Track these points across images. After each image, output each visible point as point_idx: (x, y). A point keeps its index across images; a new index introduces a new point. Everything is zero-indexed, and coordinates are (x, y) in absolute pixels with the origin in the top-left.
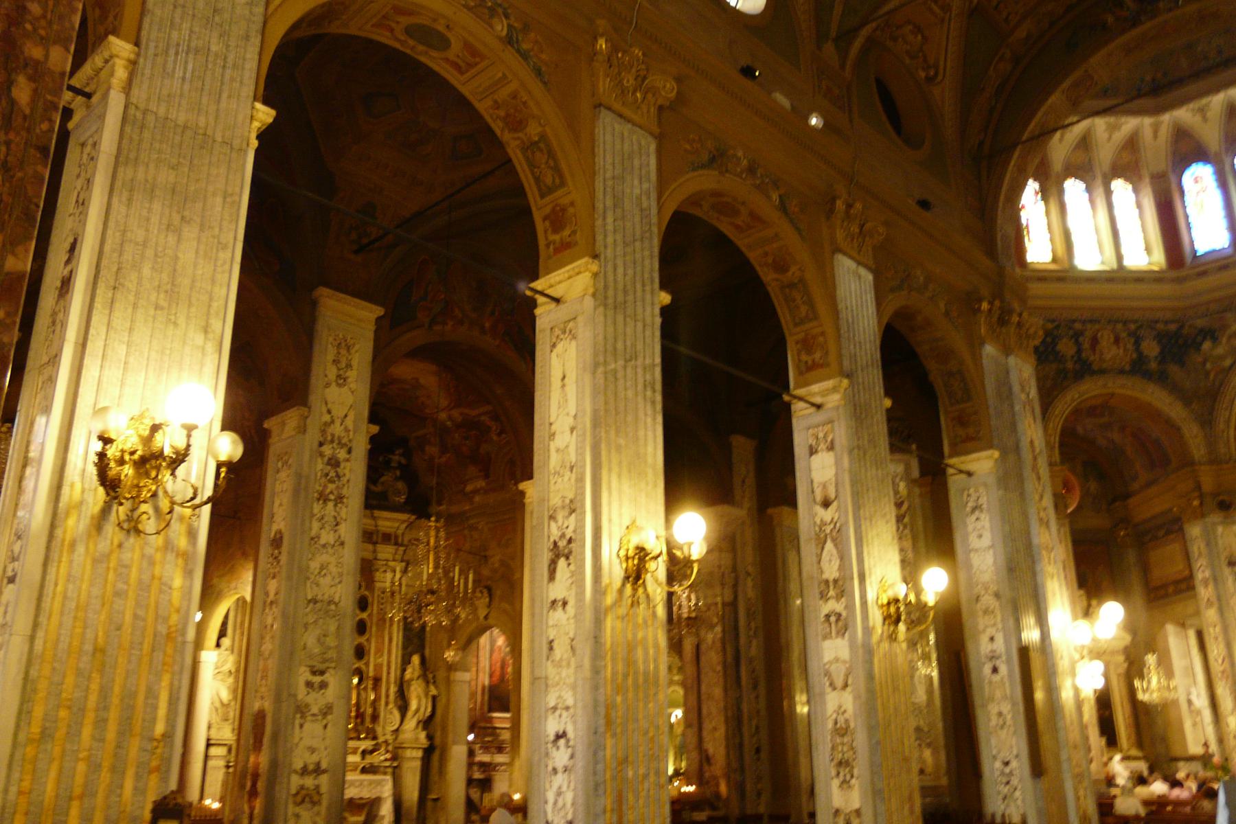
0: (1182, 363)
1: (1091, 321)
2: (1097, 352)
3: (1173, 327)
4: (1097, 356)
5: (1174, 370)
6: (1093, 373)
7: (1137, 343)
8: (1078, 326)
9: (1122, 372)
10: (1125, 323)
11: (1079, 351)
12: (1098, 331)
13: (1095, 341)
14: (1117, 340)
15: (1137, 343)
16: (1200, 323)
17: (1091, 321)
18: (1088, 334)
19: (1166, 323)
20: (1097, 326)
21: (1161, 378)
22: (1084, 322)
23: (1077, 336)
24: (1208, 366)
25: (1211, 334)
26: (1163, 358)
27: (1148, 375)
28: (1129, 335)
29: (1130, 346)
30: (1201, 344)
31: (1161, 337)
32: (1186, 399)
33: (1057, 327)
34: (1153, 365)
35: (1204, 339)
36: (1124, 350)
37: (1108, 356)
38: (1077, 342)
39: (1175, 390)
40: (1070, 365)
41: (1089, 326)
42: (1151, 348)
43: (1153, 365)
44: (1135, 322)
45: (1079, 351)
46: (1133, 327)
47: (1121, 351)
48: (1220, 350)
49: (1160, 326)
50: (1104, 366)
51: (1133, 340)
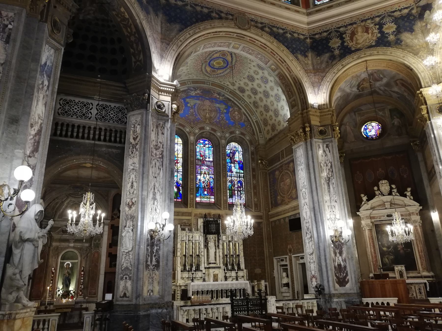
1: (351, 24)
2: (354, 39)
4: (354, 42)
8: (341, 29)
9: (370, 47)
10: (372, 19)
13: (353, 34)
17: (351, 24)
18: (349, 32)
20: (354, 26)
22: (346, 26)
26: (398, 32)
29: (376, 31)
33: (329, 34)
36: (372, 34)
37: (360, 41)
41: (349, 27)
44: (378, 16)
45: (343, 42)
47: (370, 35)
49: (397, 14)
50: (359, 46)
51: (377, 27)
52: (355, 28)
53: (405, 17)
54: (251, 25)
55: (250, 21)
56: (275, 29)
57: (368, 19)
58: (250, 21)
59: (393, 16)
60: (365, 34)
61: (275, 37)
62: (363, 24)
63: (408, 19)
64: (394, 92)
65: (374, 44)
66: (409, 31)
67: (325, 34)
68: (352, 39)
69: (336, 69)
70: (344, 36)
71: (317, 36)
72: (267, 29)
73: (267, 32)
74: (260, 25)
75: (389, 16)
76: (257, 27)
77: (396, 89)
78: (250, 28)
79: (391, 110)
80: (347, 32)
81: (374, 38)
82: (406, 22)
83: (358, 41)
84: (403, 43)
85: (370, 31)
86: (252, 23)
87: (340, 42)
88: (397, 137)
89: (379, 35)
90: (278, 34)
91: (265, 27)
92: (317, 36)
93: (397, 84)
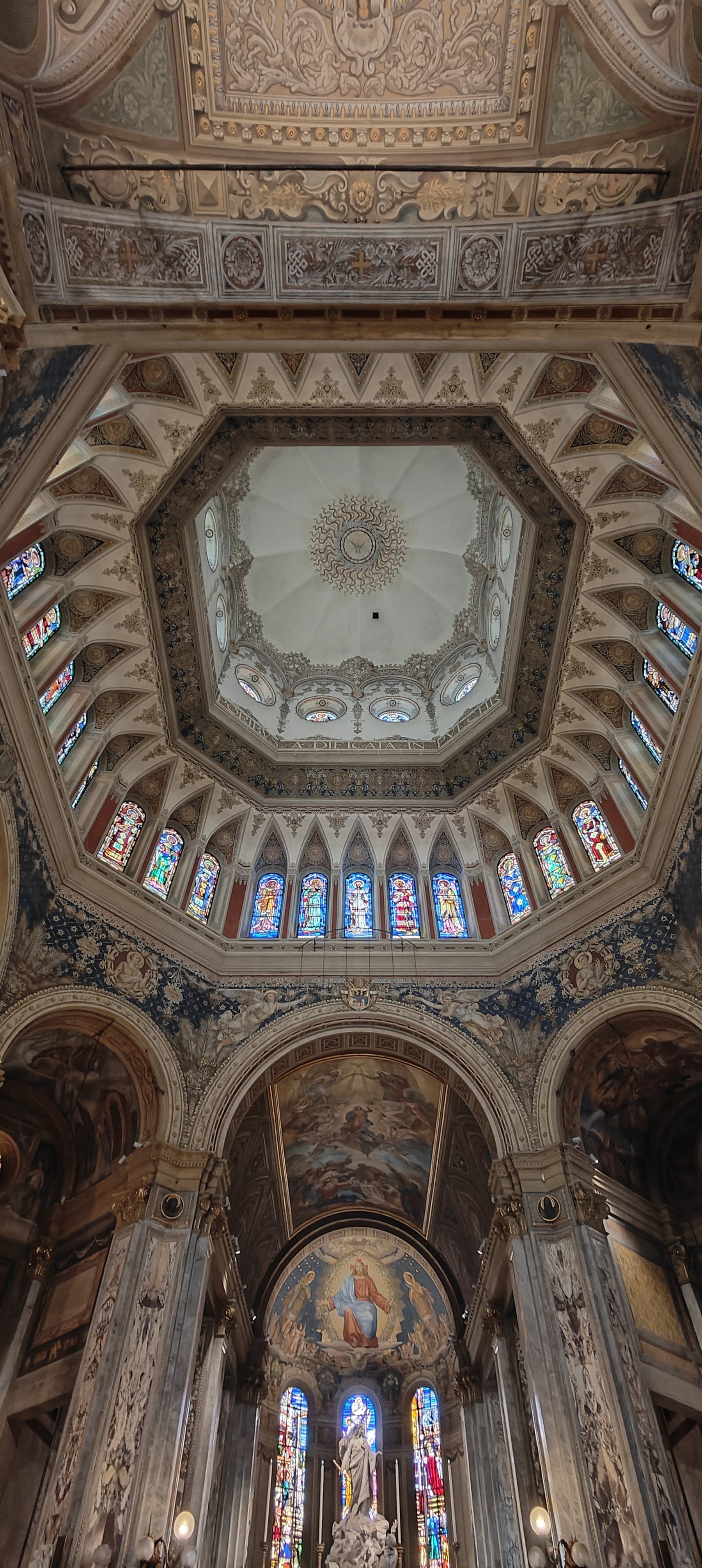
0: (196, 1025)
2: (120, 967)
3: (204, 986)
5: (186, 1025)
6: (102, 985)
7: (163, 983)
8: (112, 933)
9: (134, 1001)
10: (161, 958)
11: (100, 957)
12: (131, 950)
13: (122, 957)
14: (143, 970)
15: (163, 983)
16: (228, 993)
19: (199, 979)
21: (171, 1029)
22: (121, 935)
23: (105, 943)
24: (220, 1037)
25: (234, 1006)
26: (181, 1009)
27: (158, 1018)
28: (159, 971)
30: (222, 1012)
31: (187, 989)
32: (186, 1062)
33: (90, 923)
34: (168, 1012)
35: (228, 1008)
36: (148, 981)
37: (126, 978)
38: (103, 949)
39: (179, 1048)
40: (81, 965)
41: (124, 940)
42: (174, 995)
43: (168, 1012)
45: (100, 957)
46: (167, 965)
47: (145, 980)
48: (236, 1024)
50: (120, 985)
51: (160, 977)
52: (131, 950)
53: (199, 995)
54: (9, 788)
55: (13, 780)
56: (30, 834)
57: (156, 953)
58: (13, 780)
59: (185, 978)
60: (139, 973)
61: (20, 847)
62: (144, 952)
63: (202, 1000)
64: (83, 1111)
65: (141, 1000)
66: (192, 1021)
67: (84, 917)
68: (116, 963)
69: (61, 996)
70: (109, 947)
71: (69, 909)
72: (22, 820)
73: (18, 825)
74: (19, 803)
75: (183, 974)
76: (14, 800)
77: (91, 1107)
78: (4, 791)
79: (42, 1145)
80: (117, 945)
81: (147, 992)
82: (197, 1003)
83: (122, 976)
84: (177, 1034)
85: (147, 975)
86: (14, 788)
87: (97, 953)
88: (16, 1216)
89: (155, 992)
90: (29, 847)
91: (23, 814)
92: (69, 909)
93: (102, 1100)
